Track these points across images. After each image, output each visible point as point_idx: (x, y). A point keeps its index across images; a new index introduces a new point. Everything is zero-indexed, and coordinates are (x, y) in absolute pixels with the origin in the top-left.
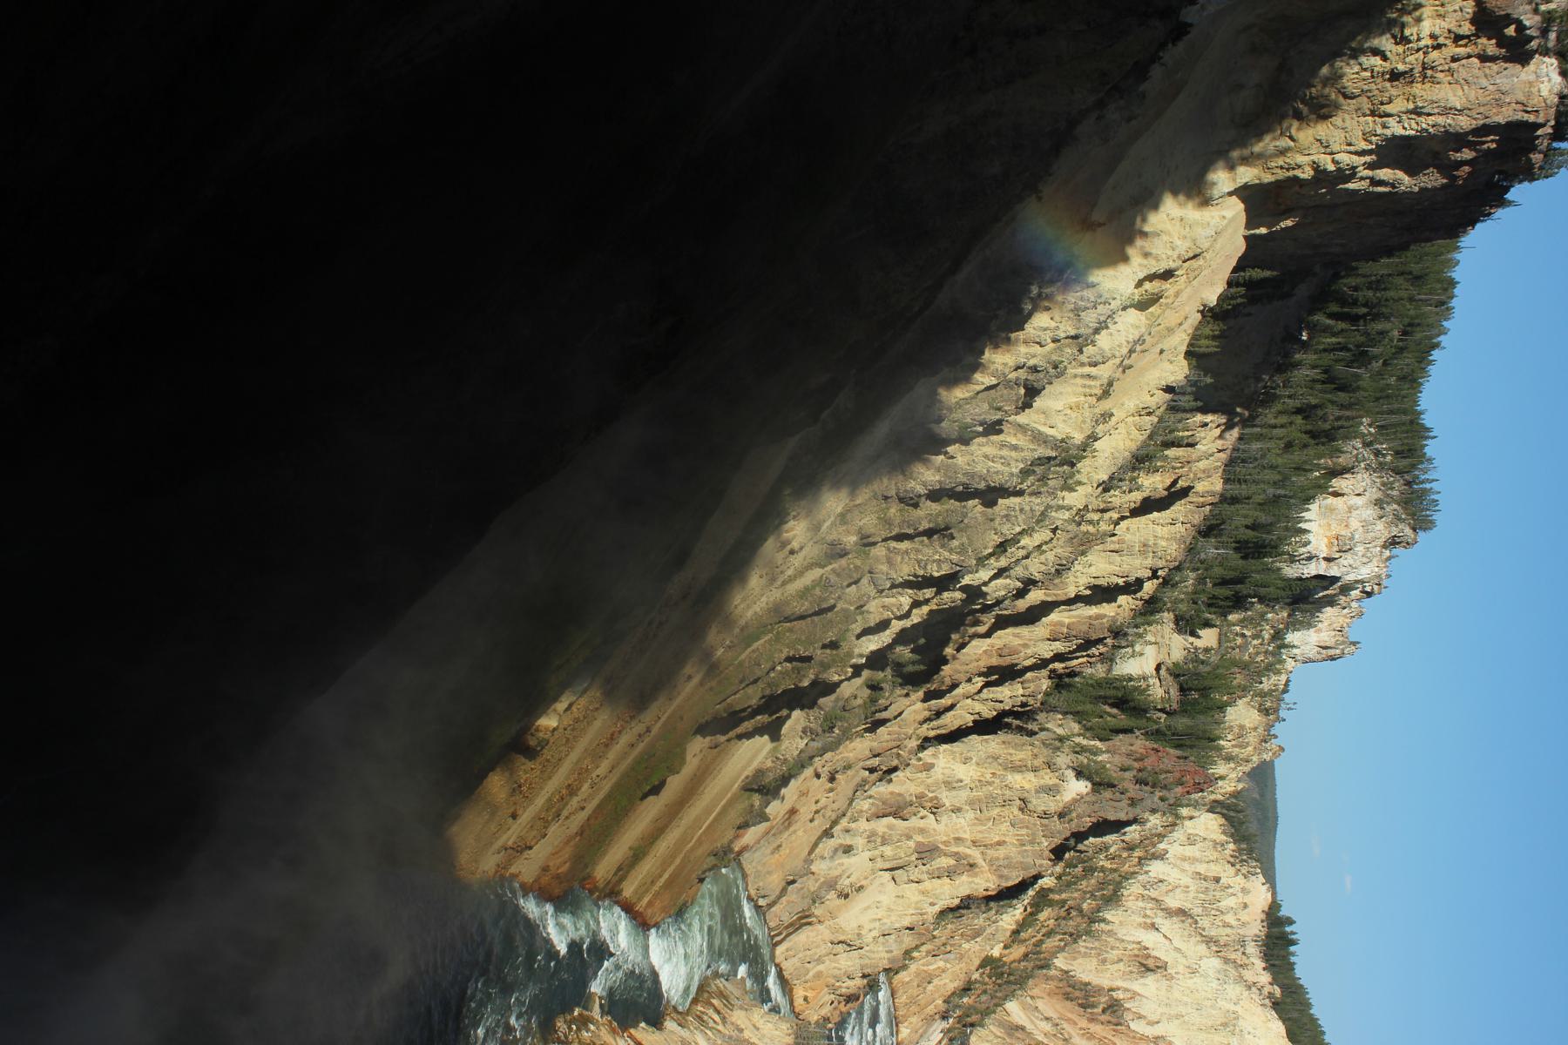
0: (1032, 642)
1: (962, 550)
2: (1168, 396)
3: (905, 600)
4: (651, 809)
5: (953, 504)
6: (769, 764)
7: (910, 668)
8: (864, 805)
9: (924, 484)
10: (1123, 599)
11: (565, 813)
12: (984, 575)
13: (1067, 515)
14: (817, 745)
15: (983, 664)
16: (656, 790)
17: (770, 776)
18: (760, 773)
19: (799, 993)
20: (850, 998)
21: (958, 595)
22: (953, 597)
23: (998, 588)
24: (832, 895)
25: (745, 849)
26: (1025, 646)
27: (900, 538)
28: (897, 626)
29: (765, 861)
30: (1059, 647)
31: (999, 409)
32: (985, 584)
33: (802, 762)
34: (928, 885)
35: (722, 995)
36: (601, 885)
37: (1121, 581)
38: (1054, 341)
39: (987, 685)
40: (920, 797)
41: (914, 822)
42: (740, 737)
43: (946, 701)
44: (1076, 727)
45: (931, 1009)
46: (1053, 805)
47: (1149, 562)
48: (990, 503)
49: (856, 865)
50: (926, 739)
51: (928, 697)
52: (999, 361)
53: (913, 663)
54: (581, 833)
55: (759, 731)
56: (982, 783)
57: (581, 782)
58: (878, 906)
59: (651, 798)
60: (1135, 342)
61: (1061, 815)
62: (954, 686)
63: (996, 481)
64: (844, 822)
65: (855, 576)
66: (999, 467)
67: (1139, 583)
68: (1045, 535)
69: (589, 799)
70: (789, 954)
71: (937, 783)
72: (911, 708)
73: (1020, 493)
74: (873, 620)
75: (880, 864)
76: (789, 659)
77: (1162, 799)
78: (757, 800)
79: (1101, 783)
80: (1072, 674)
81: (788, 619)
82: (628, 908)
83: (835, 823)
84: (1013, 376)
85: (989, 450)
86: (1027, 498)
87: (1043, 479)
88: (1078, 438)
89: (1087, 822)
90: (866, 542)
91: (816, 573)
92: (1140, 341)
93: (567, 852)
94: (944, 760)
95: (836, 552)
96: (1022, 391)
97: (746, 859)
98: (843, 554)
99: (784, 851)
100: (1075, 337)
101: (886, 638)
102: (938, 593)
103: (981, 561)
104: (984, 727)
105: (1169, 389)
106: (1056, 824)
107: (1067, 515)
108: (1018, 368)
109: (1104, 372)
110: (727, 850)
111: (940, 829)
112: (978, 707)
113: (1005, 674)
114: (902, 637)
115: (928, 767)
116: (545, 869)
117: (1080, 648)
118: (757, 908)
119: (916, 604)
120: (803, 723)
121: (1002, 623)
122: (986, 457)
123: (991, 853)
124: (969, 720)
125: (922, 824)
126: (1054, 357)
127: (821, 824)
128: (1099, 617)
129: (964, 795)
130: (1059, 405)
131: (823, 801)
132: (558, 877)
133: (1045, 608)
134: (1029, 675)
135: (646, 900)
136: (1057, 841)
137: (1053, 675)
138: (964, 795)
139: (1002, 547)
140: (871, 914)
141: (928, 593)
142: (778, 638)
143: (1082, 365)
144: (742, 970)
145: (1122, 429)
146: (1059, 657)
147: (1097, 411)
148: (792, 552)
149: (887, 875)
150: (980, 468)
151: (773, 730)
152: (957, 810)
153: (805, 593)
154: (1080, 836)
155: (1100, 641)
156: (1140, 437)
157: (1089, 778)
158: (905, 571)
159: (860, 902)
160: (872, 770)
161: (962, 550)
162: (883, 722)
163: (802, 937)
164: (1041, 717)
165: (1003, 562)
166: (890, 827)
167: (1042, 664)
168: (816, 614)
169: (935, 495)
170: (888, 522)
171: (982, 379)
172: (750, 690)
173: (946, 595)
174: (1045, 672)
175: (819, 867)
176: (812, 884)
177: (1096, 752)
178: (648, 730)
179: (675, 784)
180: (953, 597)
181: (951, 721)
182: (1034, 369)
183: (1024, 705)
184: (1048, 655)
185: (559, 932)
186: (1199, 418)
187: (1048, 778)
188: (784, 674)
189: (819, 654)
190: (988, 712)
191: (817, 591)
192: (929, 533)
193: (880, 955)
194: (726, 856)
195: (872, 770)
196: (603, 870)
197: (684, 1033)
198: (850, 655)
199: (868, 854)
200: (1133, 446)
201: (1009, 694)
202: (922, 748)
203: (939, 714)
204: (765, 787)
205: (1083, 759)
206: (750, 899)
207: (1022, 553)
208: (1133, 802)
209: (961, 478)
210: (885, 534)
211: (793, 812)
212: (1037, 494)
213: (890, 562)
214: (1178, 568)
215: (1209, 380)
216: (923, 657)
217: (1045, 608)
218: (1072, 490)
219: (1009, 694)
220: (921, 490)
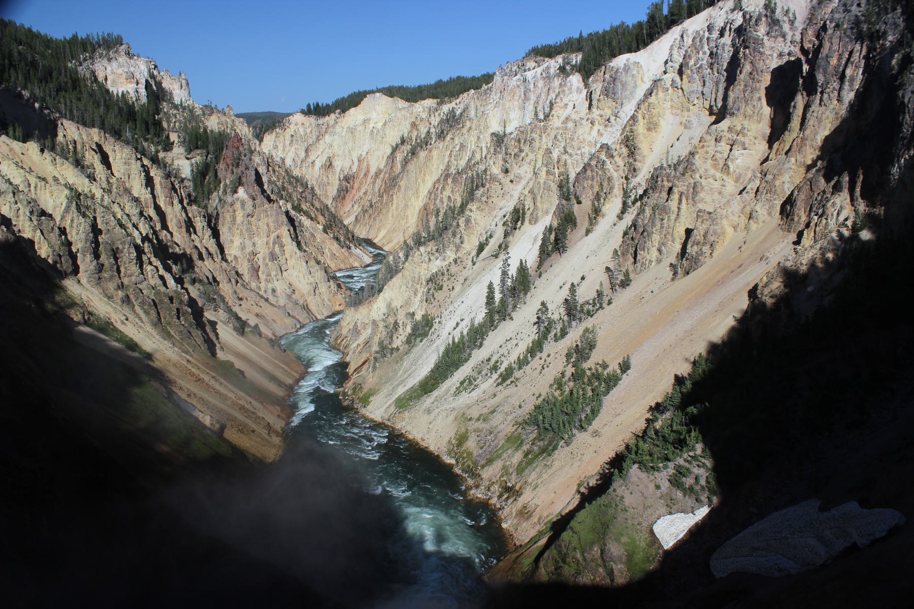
0: (174, 213)
1: (123, 243)
2: (46, 151)
3: (149, 268)
4: (250, 373)
5: (101, 248)
6: (231, 325)
7: (185, 266)
8: (254, 285)
9: (92, 261)
10: (152, 174)
11: (253, 410)
12: (136, 234)
13: (106, 197)
14: (222, 306)
15: (185, 235)
16: (242, 372)
17: (237, 324)
18: (235, 329)
19: (338, 308)
20: (339, 286)
21: (146, 244)
22: (147, 247)
23: (144, 228)
24: (294, 296)
25: (274, 334)
26: (176, 216)
27: (119, 272)
28: (162, 271)
29: (282, 326)
30: (176, 201)
31: (53, 229)
32: (140, 233)
33: (229, 310)
34: (287, 256)
35: (336, 339)
36: (287, 393)
37: (143, 174)
38: (16, 203)
39: (195, 233)
40: (249, 261)
41: (260, 263)
42: (218, 338)
43: (204, 252)
44: (215, 194)
45: (346, 254)
46: (250, 203)
47: (133, 161)
48: (100, 232)
49: (280, 286)
50: (222, 259)
51: (201, 258)
52: (27, 229)
53: (182, 264)
54: (262, 403)
55: (215, 330)
56: (242, 234)
57: (237, 404)
58: (298, 277)
59: (246, 374)
60: (17, 166)
61: (254, 199)
62: (196, 247)
63: (89, 229)
64: (262, 293)
65: (138, 290)
66: (82, 228)
67: (143, 166)
68: (116, 208)
69: (246, 400)
70: (321, 313)
71: (243, 254)
72: (205, 267)
73: (95, 218)
74: (160, 282)
75: (279, 276)
76: (179, 318)
77: (245, 156)
78: (247, 330)
79: (239, 182)
80: (189, 195)
81: (160, 319)
82: (298, 381)
83: (262, 297)
84: (35, 223)
85: (74, 232)
86: (97, 215)
87: (88, 208)
88: (67, 192)
89: (257, 188)
90: (121, 286)
91: (137, 308)
92: (17, 164)
93: (271, 407)
94: (232, 251)
95: (127, 300)
96: (43, 218)
97: (279, 334)
98: (128, 297)
99: (275, 318)
100: (14, 193)
101: (168, 276)
102: (145, 254)
103: (129, 235)
104: (216, 234)
105: (42, 151)
106: (258, 201)
107: (106, 197)
108: (31, 220)
109: (33, 180)
110: (271, 340)
111: (263, 251)
112: (207, 237)
113: (189, 226)
114: (168, 269)
115: (236, 258)
116: (279, 416)
117: (176, 192)
118: (301, 327)
119: (150, 263)
120: (212, 312)
121: (165, 226)
122: (77, 234)
123: (272, 229)
124: (213, 241)
125: (261, 260)
126: (25, 203)
127: (262, 303)
128: (161, 184)
129: (247, 242)
130: (51, 201)
131: (252, 302)
132: (282, 411)
133: (157, 208)
134: (190, 215)
135: (295, 374)
136: (265, 201)
137: (190, 203)
138: (247, 242)
139: (122, 226)
140: (302, 279)
141: (144, 258)
142: (169, 324)
143: (30, 190)
144: (328, 332)
145: (63, 172)
146: (181, 202)
147: (53, 183)
148: (127, 319)
149: (284, 273)
150: (83, 236)
151: (213, 324)
152: (254, 244)
153: (147, 313)
154: (263, 192)
155: (172, 184)
156: (67, 164)
157: (237, 188)
158: (135, 269)
159: (296, 284)
160: (237, 282)
161: (123, 243)
162: (214, 279)
163: (313, 308)
164: (210, 210)
165: (130, 225)
166: (263, 273)
167: (184, 208)
168: (156, 307)
169: (97, 256)
170: (112, 277)
171: (38, 237)
172: (194, 334)
173: (146, 250)
174: (188, 208)
175: (282, 302)
176: (290, 305)
177: (226, 185)
178: (214, 377)
179: (238, 364)
180: (147, 247)
181: (213, 248)
182: (32, 213)
183: (204, 217)
184: (180, 206)
185: (307, 408)
186: (60, 138)
187: (238, 205)
188: (186, 320)
189: (176, 305)
190: (208, 232)
191: (146, 307)
192: (116, 259)
193: (319, 275)
194: (274, 342)
195: (237, 282)
196: (280, 392)
197: (351, 353)
198: (176, 291)
199: (276, 282)
200: (72, 167)
201: (200, 223)
202: (226, 261)
203: (210, 254)
204: (241, 327)
205: (229, 190)
206: (297, 331)
207: (125, 217)
208: (247, 168)
209: (88, 244)
210: (117, 278)
211: (257, 315)
212: (95, 210)
213: (130, 276)
214: (136, 149)
215: (37, 132)
216: (181, 263)
217: (157, 208)
218: (93, 197)
219: (200, 223)
220: (95, 262)
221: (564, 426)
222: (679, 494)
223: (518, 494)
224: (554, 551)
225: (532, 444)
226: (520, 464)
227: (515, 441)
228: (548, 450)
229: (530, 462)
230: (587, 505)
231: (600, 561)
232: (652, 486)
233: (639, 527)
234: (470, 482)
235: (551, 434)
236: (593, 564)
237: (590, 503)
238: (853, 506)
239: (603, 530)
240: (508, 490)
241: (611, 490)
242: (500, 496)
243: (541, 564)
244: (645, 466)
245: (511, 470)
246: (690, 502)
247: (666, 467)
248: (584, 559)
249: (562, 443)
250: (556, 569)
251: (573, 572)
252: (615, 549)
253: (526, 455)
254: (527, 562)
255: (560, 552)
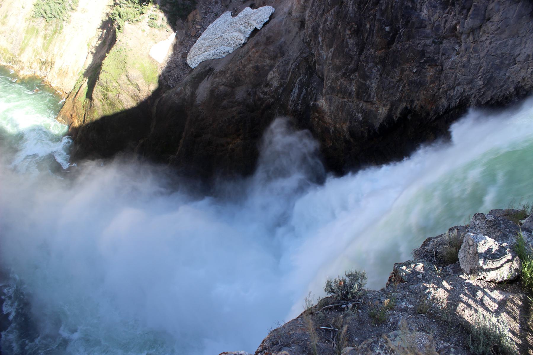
221: (61, 12)
222: (156, 31)
223: (52, 63)
224: (100, 87)
225: (46, 30)
226: (43, 46)
227: (33, 31)
228: (58, 30)
229: (50, 42)
230: (107, 55)
231: (128, 82)
232: (140, 32)
233: (142, 56)
234: (16, 67)
235: (54, 20)
236: (125, 85)
237: (108, 52)
238: (248, 10)
239: (123, 65)
240: (44, 63)
241: (118, 41)
242: (41, 69)
243: (94, 96)
244: (133, 22)
245: (40, 51)
246: (163, 33)
247: (143, 18)
248: (119, 85)
249: (64, 23)
250: (104, 96)
251: (115, 94)
252: (134, 73)
253: (45, 38)
254: (82, 98)
255: (102, 87)
